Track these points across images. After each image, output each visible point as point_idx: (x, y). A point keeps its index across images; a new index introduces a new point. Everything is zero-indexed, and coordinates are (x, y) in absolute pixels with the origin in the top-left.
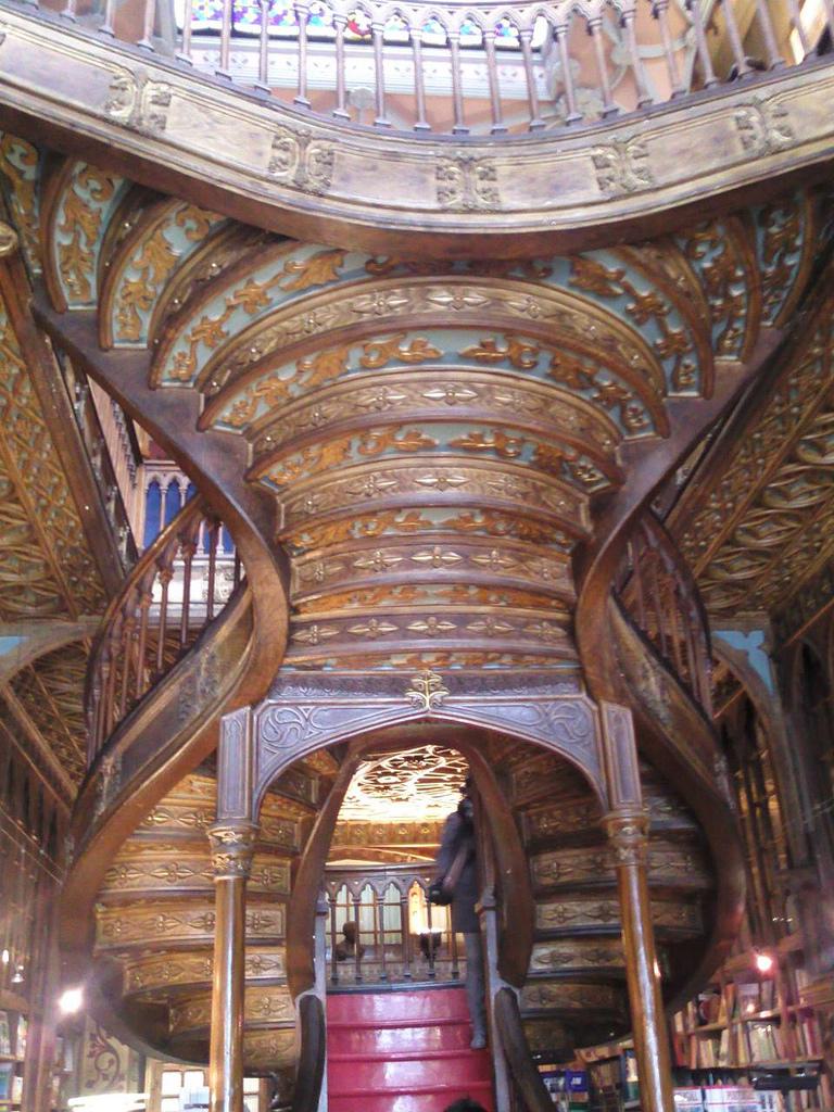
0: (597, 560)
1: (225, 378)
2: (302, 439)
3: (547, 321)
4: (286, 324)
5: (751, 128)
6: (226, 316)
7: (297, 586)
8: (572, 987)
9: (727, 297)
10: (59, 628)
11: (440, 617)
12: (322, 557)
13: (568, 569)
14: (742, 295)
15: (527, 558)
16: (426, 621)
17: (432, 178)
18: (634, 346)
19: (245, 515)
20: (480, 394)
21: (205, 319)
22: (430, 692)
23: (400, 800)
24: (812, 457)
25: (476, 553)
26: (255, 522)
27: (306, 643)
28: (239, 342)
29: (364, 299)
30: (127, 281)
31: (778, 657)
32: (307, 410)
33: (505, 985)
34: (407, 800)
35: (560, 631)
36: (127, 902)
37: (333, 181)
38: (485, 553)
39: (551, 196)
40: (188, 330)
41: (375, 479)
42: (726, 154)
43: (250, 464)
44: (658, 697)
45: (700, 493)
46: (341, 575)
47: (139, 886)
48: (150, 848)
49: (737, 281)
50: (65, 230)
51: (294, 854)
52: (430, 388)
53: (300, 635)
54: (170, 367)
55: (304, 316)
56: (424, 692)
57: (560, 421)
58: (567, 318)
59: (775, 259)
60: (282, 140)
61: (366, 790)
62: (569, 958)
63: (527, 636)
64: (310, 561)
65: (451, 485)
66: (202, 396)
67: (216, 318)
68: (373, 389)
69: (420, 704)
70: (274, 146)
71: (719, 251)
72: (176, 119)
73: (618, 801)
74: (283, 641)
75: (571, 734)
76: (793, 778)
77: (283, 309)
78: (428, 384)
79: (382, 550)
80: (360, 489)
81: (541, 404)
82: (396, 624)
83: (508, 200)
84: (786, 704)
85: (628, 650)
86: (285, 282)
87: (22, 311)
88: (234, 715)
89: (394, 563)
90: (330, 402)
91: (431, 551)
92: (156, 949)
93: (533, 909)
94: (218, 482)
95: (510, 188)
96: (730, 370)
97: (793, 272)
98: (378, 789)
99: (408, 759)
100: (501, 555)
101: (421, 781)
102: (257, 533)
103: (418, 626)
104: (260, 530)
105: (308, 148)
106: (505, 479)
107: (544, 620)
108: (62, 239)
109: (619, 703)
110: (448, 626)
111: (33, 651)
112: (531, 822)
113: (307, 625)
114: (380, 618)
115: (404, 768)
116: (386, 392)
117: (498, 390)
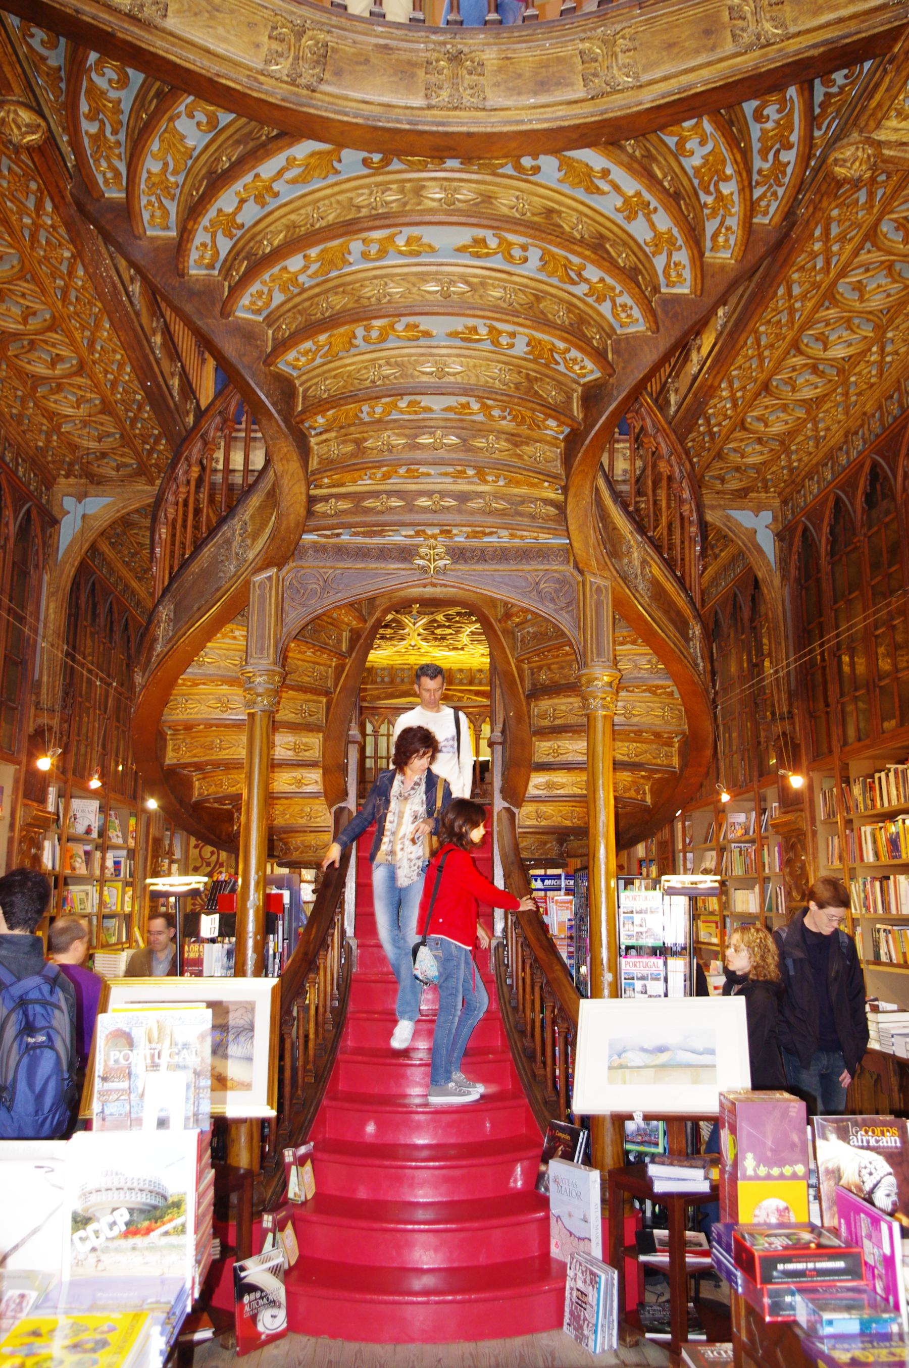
0: (584, 447)
1: (243, 269)
2: (311, 329)
3: (536, 219)
4: (293, 217)
5: (744, 19)
6: (239, 209)
7: (315, 463)
8: (566, 809)
9: (720, 197)
10: (138, 491)
11: (443, 494)
12: (336, 438)
14: (732, 194)
15: (522, 443)
17: (421, 73)
18: (625, 244)
19: (263, 397)
20: (473, 288)
21: (220, 211)
22: (435, 560)
23: (455, 649)
24: (816, 350)
25: (475, 437)
26: (273, 404)
27: (325, 515)
28: (253, 233)
29: (363, 194)
30: (149, 172)
31: (782, 536)
32: (316, 300)
33: (507, 805)
34: (462, 649)
35: (552, 510)
36: (189, 727)
37: (327, 76)
38: (483, 437)
39: (535, 93)
40: (205, 221)
41: (380, 366)
42: (713, 48)
43: (269, 350)
44: (639, 571)
45: (709, 383)
46: (353, 455)
47: (197, 713)
48: (204, 684)
49: (727, 179)
50: (91, 118)
51: (327, 693)
52: (427, 282)
53: (319, 507)
54: (194, 255)
55: (309, 209)
56: (429, 560)
57: (550, 316)
58: (555, 216)
59: (771, 156)
60: (279, 30)
61: (425, 639)
62: (562, 786)
63: (521, 514)
64: (325, 441)
65: (448, 374)
66: (226, 284)
67: (229, 210)
68: (375, 281)
69: (424, 570)
70: (270, 37)
71: (709, 147)
72: (176, 6)
73: (592, 660)
74: (303, 512)
76: (783, 644)
77: (291, 202)
78: (423, 277)
79: (389, 433)
80: (366, 376)
81: (532, 298)
82: (403, 499)
83: (495, 99)
84: (784, 577)
86: (289, 175)
87: (63, 197)
89: (399, 445)
90: (336, 293)
91: (432, 434)
92: (217, 764)
93: (530, 744)
94: (240, 367)
95: (497, 84)
96: (723, 267)
97: (789, 170)
98: (436, 639)
99: (458, 614)
100: (497, 438)
101: (472, 633)
102: (276, 415)
103: (423, 502)
104: (278, 412)
105: (303, 40)
106: (500, 370)
107: (537, 499)
108: (89, 127)
110: (450, 502)
111: (118, 511)
112: (533, 674)
113: (325, 499)
114: (390, 494)
116: (386, 284)
117: (492, 285)
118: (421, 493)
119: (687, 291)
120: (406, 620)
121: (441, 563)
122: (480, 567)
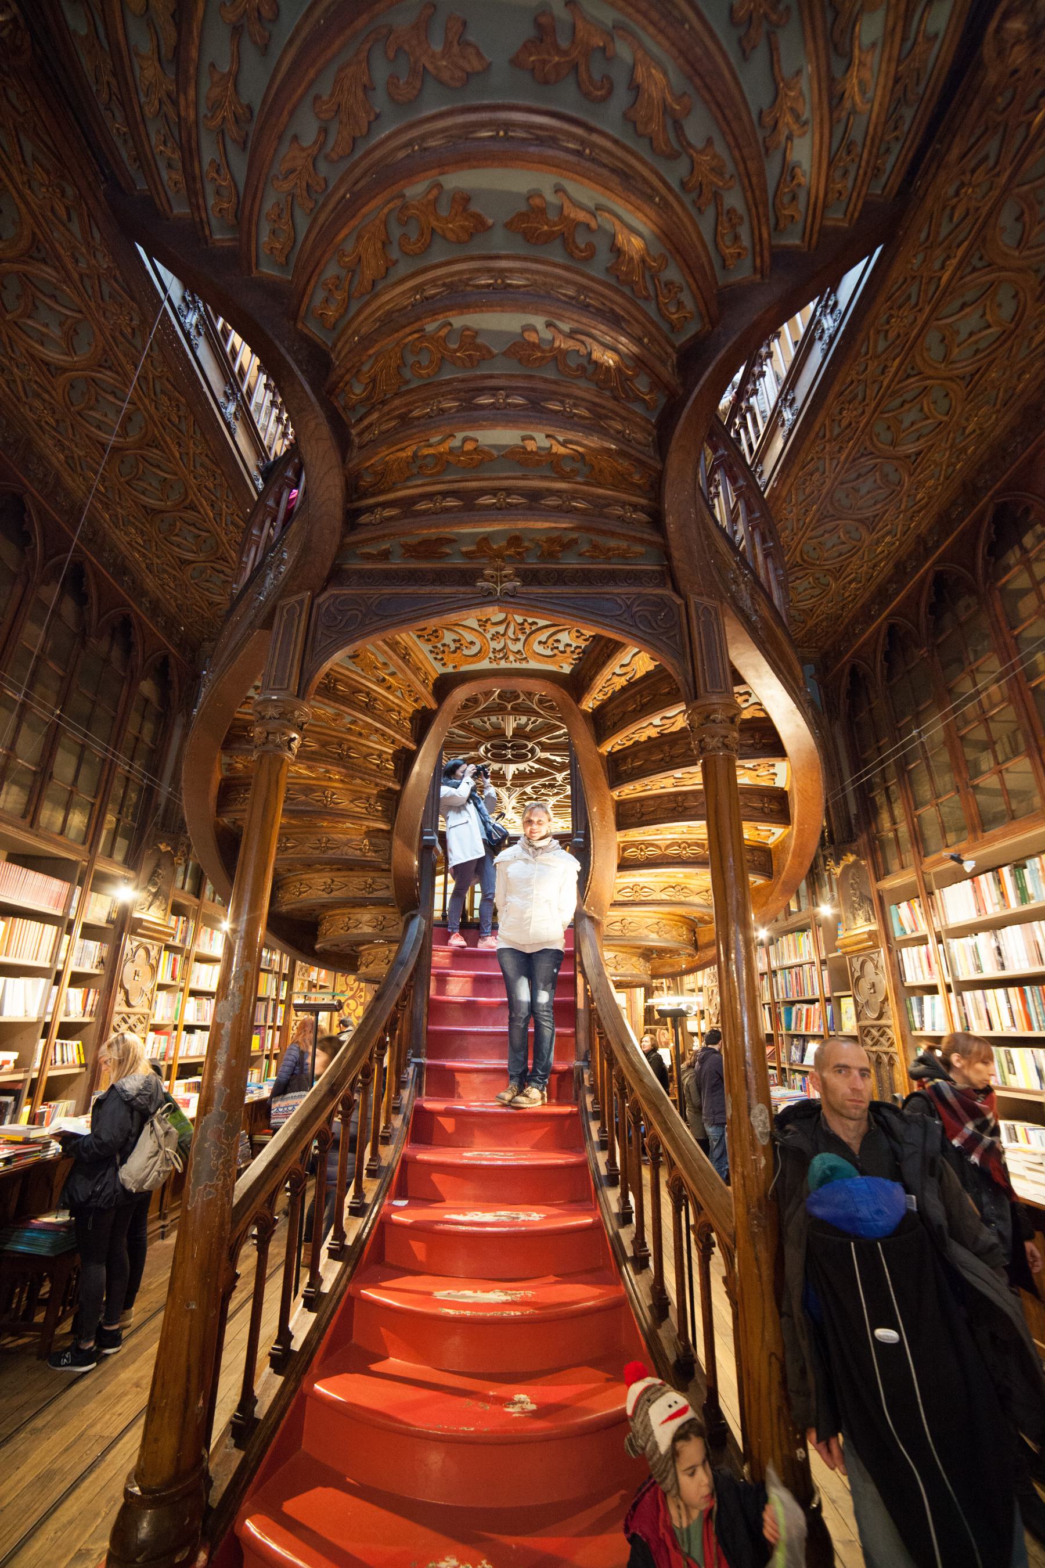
11: (509, 491)
12: (379, 418)
13: (653, 441)
16: (495, 495)
19: (283, 350)
22: (502, 582)
53: (364, 519)
56: (496, 583)
73: (706, 691)
75: (654, 624)
82: (460, 499)
85: (717, 552)
88: (293, 599)
89: (450, 408)
99: (544, 786)
103: (487, 500)
109: (709, 596)
113: (370, 509)
114: (445, 494)
115: (543, 794)
118: (483, 492)
119: (797, 242)
120: (503, 793)
121: (508, 585)
122: (557, 590)
